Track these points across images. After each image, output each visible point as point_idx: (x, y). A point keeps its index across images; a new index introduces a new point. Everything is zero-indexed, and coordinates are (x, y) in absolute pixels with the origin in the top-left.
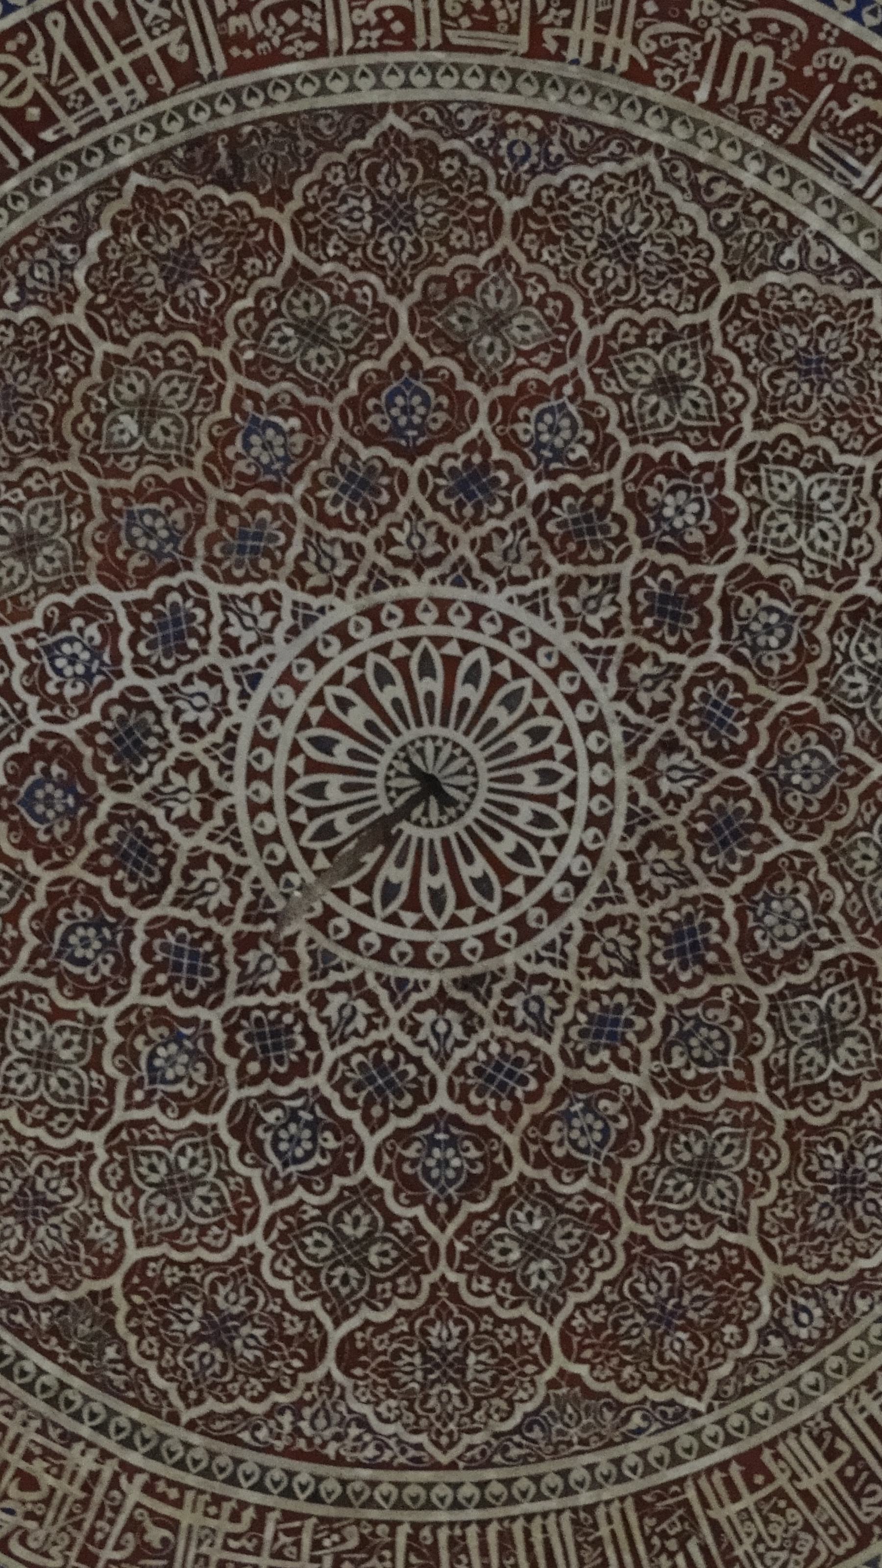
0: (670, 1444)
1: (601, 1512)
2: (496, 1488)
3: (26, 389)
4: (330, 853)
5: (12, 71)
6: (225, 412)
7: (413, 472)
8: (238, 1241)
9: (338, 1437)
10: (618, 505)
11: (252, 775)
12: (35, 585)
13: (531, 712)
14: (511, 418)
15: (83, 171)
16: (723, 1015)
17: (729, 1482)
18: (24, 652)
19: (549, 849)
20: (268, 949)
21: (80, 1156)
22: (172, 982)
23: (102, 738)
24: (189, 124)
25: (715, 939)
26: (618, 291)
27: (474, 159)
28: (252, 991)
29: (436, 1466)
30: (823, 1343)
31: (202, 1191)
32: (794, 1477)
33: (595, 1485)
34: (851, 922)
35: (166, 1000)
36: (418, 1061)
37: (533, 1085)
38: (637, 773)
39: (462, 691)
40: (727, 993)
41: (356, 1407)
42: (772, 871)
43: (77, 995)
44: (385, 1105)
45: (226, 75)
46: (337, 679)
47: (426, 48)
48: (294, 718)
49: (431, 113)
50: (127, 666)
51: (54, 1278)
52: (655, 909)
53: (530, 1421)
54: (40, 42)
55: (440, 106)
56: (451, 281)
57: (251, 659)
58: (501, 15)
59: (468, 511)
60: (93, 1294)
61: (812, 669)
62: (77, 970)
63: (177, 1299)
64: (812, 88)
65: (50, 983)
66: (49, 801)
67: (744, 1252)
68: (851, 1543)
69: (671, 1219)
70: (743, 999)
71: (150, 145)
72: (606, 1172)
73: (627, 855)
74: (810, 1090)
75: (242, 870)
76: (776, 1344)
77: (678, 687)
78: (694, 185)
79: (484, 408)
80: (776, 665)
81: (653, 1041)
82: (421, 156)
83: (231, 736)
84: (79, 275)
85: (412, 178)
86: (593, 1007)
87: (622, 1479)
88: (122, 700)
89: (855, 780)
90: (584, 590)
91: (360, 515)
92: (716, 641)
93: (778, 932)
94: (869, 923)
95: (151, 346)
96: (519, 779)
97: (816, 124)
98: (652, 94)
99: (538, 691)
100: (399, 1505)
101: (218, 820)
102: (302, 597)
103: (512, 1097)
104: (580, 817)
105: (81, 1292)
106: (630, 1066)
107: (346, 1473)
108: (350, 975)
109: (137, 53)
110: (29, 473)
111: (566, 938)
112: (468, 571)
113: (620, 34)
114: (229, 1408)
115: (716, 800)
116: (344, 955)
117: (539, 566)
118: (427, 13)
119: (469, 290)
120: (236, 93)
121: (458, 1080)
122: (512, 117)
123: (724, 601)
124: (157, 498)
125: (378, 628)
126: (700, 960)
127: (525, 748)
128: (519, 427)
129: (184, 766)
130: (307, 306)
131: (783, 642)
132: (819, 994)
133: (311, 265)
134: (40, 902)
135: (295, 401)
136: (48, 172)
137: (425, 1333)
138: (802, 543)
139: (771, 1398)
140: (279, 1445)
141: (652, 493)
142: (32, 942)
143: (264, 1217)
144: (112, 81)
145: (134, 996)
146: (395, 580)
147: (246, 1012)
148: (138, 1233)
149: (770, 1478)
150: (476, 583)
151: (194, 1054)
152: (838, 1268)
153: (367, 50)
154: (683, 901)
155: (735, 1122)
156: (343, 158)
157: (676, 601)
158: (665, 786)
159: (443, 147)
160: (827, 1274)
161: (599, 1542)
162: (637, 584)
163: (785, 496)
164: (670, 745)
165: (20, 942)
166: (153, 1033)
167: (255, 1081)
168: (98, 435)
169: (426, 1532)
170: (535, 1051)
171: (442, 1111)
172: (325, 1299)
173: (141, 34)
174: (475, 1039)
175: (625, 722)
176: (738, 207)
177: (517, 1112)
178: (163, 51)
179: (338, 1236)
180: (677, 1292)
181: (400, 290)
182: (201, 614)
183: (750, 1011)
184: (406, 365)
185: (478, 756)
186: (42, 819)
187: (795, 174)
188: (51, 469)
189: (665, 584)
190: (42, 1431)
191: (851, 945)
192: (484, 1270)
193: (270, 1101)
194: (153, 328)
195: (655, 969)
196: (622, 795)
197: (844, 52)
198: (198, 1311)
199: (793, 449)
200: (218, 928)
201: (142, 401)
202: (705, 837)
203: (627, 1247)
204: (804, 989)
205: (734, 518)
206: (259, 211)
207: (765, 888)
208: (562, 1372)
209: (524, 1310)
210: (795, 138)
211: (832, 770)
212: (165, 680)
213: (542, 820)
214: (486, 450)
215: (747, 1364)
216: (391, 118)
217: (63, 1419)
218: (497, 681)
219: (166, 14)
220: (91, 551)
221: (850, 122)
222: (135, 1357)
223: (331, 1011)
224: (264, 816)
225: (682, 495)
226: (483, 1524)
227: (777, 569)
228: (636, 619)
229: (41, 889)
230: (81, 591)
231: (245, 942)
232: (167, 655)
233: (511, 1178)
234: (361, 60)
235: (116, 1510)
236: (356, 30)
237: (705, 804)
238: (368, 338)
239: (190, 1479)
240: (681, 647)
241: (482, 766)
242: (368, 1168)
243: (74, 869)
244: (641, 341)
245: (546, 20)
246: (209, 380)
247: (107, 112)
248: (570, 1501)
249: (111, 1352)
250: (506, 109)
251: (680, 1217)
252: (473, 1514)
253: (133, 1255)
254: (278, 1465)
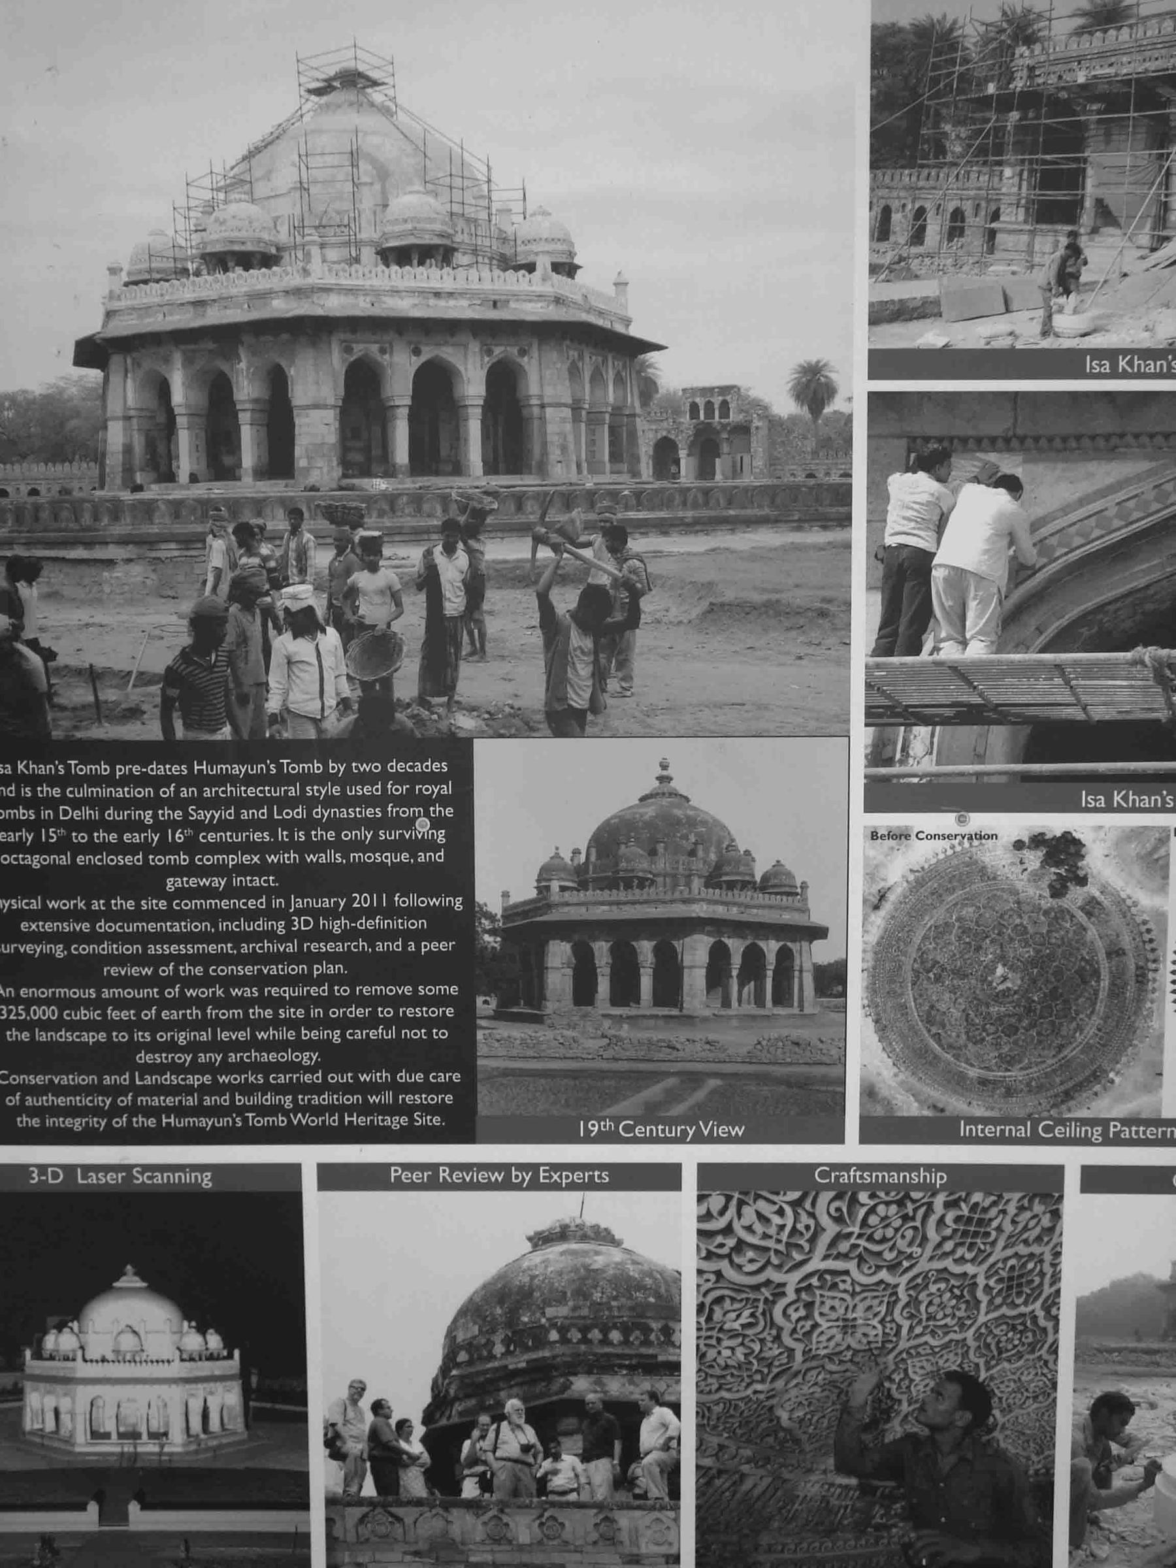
40: (916, 1250)
70: (906, 1264)
132: (882, 1322)
183: (893, 1267)
207: (968, 1297)
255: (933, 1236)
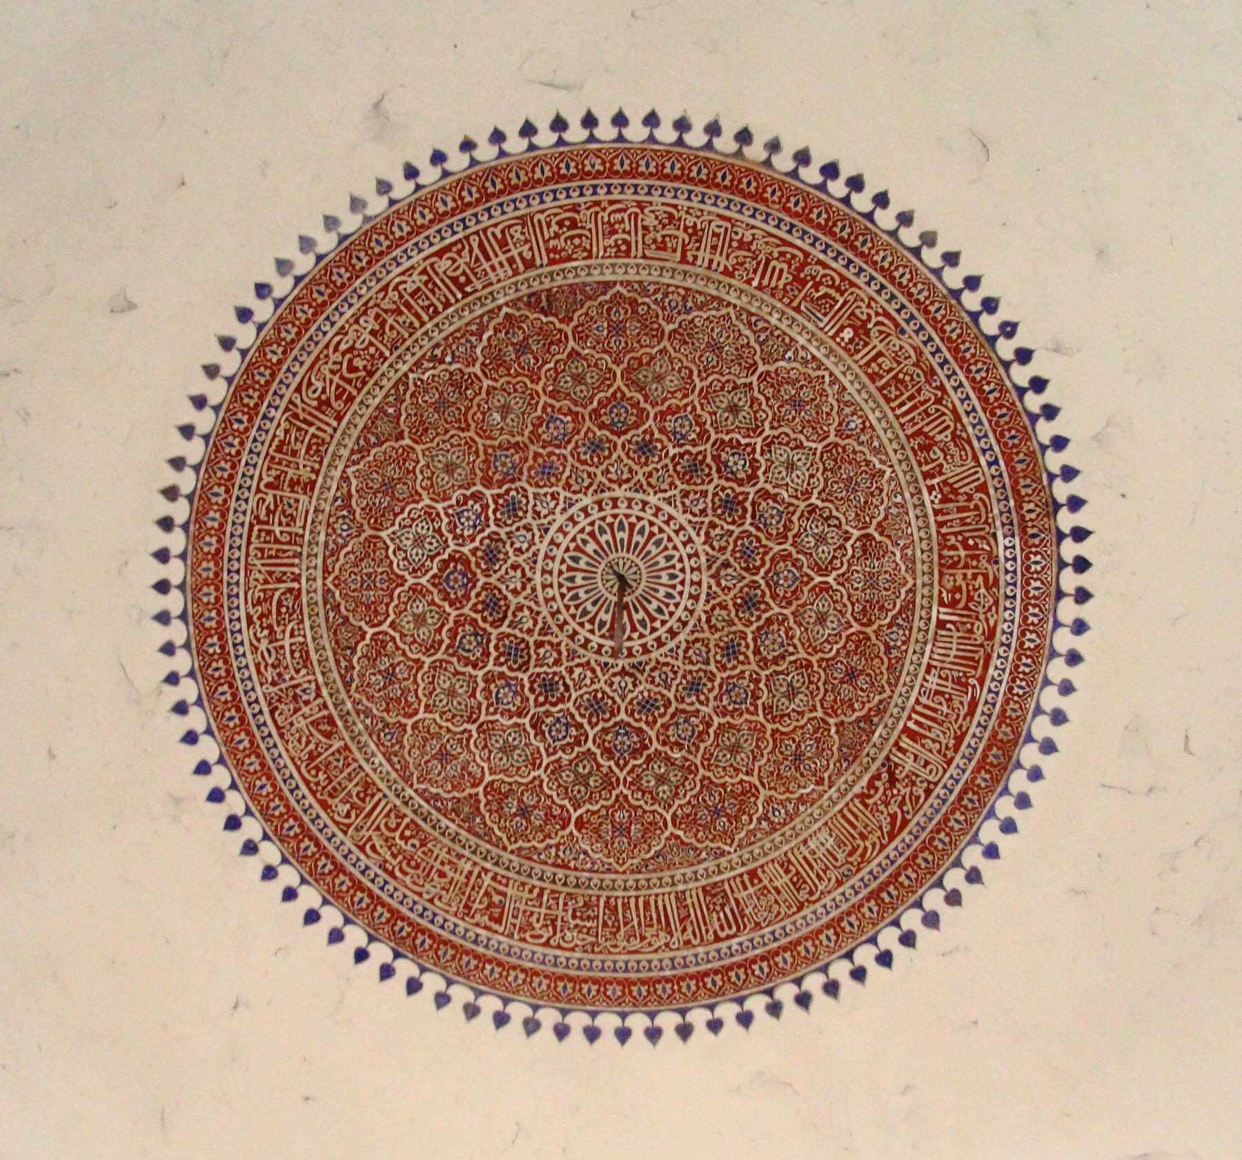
0: (718, 866)
1: (688, 894)
2: (643, 882)
3: (453, 400)
4: (577, 607)
5: (454, 261)
6: (539, 412)
7: (619, 442)
8: (533, 774)
9: (575, 859)
10: (709, 460)
11: (544, 572)
12: (453, 486)
13: (666, 548)
14: (663, 419)
15: (483, 305)
16: (746, 682)
17: (743, 882)
18: (447, 514)
19: (672, 608)
20: (548, 647)
21: (466, 735)
22: (506, 661)
23: (479, 554)
24: (529, 286)
25: (743, 649)
26: (713, 367)
27: (653, 307)
28: (542, 666)
29: (617, 872)
30: (785, 824)
31: (518, 752)
32: (771, 880)
33: (685, 882)
34: (803, 644)
35: (504, 669)
36: (613, 699)
37: (662, 710)
38: (712, 576)
39: (636, 538)
41: (583, 846)
42: (769, 621)
43: (466, 665)
44: (598, 716)
45: (548, 265)
46: (582, 531)
47: (636, 257)
48: (563, 547)
49: (636, 286)
50: (491, 522)
51: (454, 787)
52: (717, 635)
53: (658, 854)
54: (467, 248)
55: (640, 283)
56: (640, 359)
57: (545, 521)
58: (669, 245)
59: (643, 460)
60: (470, 795)
61: (790, 535)
62: (466, 654)
63: (507, 797)
64: (803, 283)
65: (454, 660)
66: (456, 580)
67: (750, 783)
68: (795, 909)
69: (720, 769)
71: (512, 295)
72: (693, 749)
73: (706, 612)
74: (782, 716)
75: (538, 613)
76: (764, 824)
77: (731, 540)
78: (749, 323)
79: (652, 415)
80: (774, 532)
81: (715, 692)
82: (630, 305)
83: (535, 555)
84: (478, 351)
85: (626, 313)
86: (689, 677)
87: (697, 880)
88: (489, 537)
89: (807, 583)
90: (692, 496)
91: (596, 460)
92: (749, 520)
93: (771, 647)
94: (810, 645)
95: (508, 383)
96: (659, 577)
97: (804, 298)
98: (733, 282)
99: (670, 539)
100: (601, 888)
101: (529, 591)
102: (569, 495)
103: (653, 714)
104: (686, 595)
105: (466, 793)
106: (706, 703)
107: (578, 874)
108: (584, 660)
109: (509, 255)
110: (452, 437)
111: (678, 647)
112: (641, 486)
113: (721, 254)
114: (529, 845)
115: (746, 589)
116: (581, 651)
117: (672, 485)
118: (637, 242)
119: (648, 364)
120: (551, 273)
121: (630, 708)
122: (671, 289)
123: (753, 504)
124: (507, 449)
125: (601, 509)
126: (736, 658)
127: (663, 564)
128: (667, 424)
129: (515, 567)
130: (577, 368)
131: (778, 522)
132: (788, 675)
133: (580, 350)
134: (451, 624)
135: (569, 409)
136: (468, 305)
137: (613, 816)
138: (788, 480)
139: (762, 847)
140: (550, 861)
141: (724, 455)
142: (447, 641)
143: (545, 764)
144: (497, 266)
145: (490, 666)
146: (609, 489)
147: (538, 675)
148: (490, 769)
149: (760, 881)
150: (644, 492)
151: (516, 693)
152: (792, 792)
153: (610, 257)
154: (730, 633)
155: (749, 729)
156: (596, 303)
157: (732, 502)
158: (723, 583)
159: (640, 300)
160: (787, 795)
161: (686, 906)
162: (715, 495)
163: (782, 459)
164: (726, 565)
165: (441, 642)
166: (498, 682)
167: (542, 704)
168: (483, 421)
169: (612, 900)
170: (663, 696)
171: (622, 721)
172: (570, 799)
173: (511, 246)
174: (637, 690)
175: (707, 554)
176: (768, 333)
177: (655, 722)
178: (520, 254)
179: (576, 773)
180: (722, 801)
181: (617, 362)
182: (524, 501)
183: (757, 681)
184: (619, 395)
185: (642, 566)
186: (453, 588)
187: (794, 320)
188: (462, 435)
189: (728, 495)
190: (449, 852)
191: (802, 654)
192: (639, 789)
193: (548, 714)
194: (509, 375)
195: (717, 662)
196: (704, 586)
197: (819, 268)
198: (515, 803)
199: (786, 439)
200: (526, 637)
201: (503, 407)
202: (741, 605)
203: (701, 781)
204: (782, 673)
205: (759, 468)
206: (558, 325)
208: (672, 834)
209: (656, 807)
210: (795, 304)
211: (797, 579)
212: (508, 529)
213: (669, 596)
214: (652, 435)
215: (752, 833)
216: (618, 287)
217: (457, 848)
218: (652, 534)
219: (523, 238)
220: (478, 471)
221: (819, 298)
222: (489, 823)
223: (575, 675)
224: (549, 590)
225: (737, 457)
226: (637, 898)
227: (777, 490)
228: (714, 510)
229: (451, 619)
230: (473, 489)
231: (539, 645)
232: (509, 518)
233: (652, 750)
234: (607, 262)
235: (480, 887)
236: (605, 249)
237: (741, 591)
238: (603, 383)
239: (510, 875)
240: (734, 522)
241: (644, 571)
242: (590, 743)
243: (466, 611)
244: (722, 389)
245: (689, 247)
246: (533, 398)
247: (494, 280)
248: (675, 889)
249: (478, 820)
250: (669, 286)
251: (724, 769)
252: (633, 893)
253: (488, 778)
254: (549, 870)
255: (740, 668)
